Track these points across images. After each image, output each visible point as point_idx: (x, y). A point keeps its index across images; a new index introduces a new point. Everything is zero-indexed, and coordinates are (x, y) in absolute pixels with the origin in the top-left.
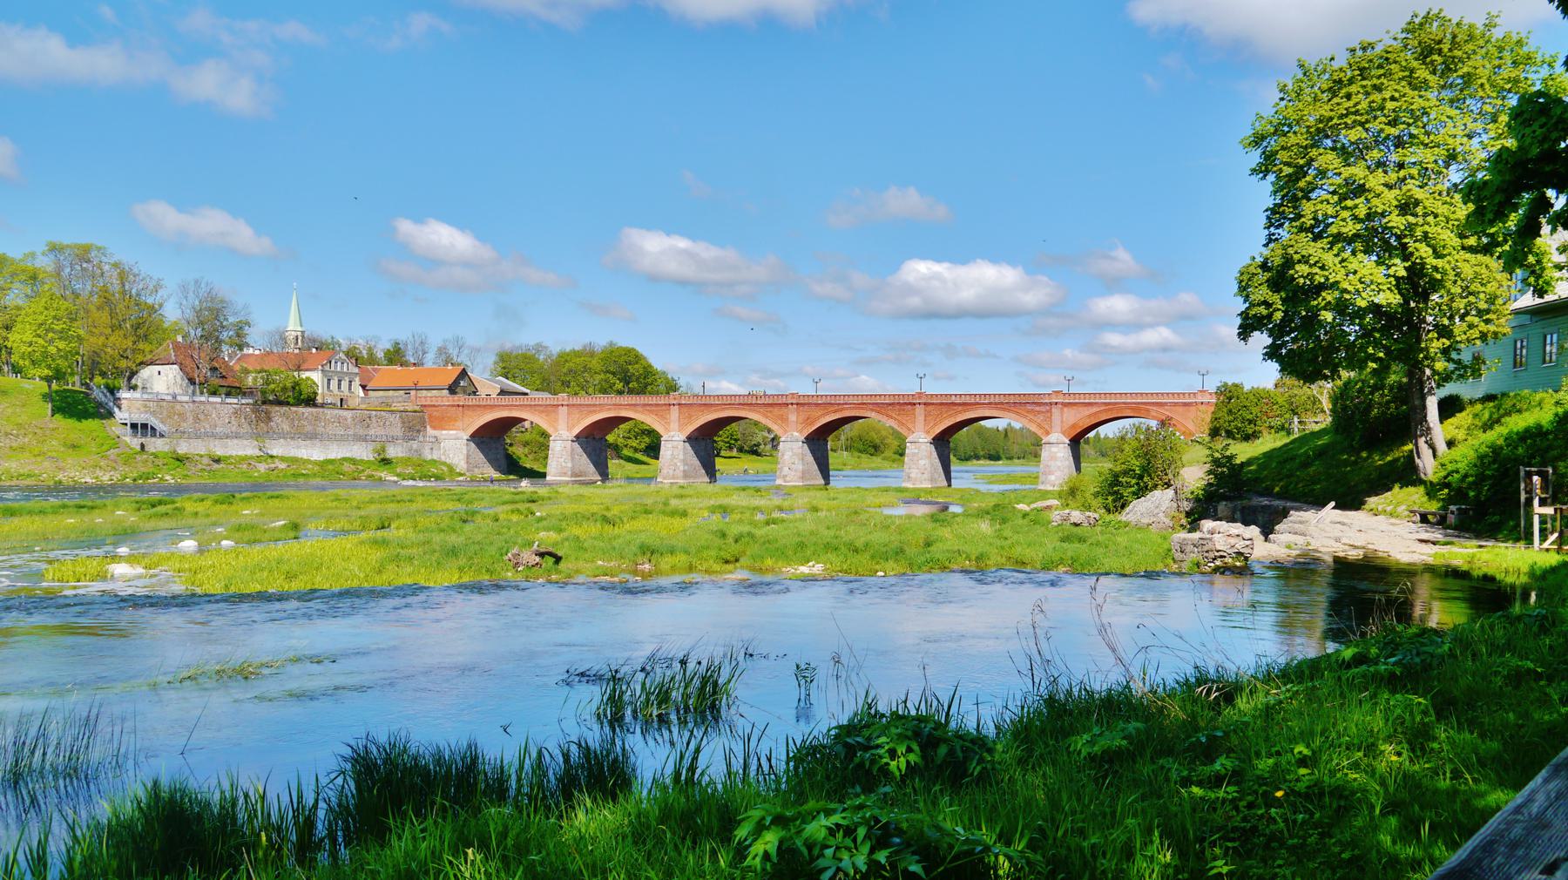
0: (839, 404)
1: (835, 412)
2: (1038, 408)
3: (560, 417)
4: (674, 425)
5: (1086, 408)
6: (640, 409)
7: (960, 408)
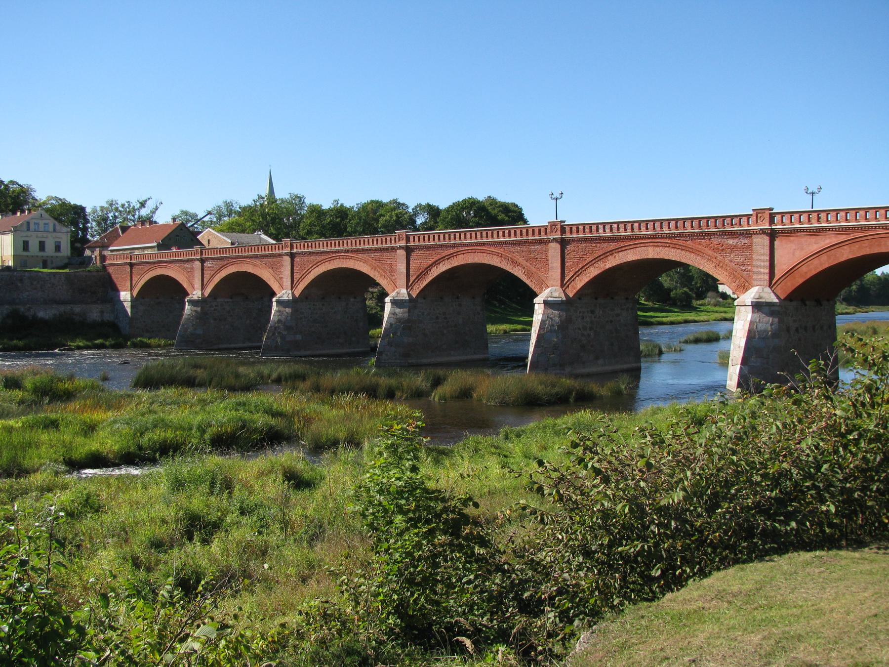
0: (454, 246)
1: (450, 256)
2: (731, 242)
3: (196, 275)
4: (287, 282)
5: (812, 240)
6: (257, 262)
7: (613, 246)
